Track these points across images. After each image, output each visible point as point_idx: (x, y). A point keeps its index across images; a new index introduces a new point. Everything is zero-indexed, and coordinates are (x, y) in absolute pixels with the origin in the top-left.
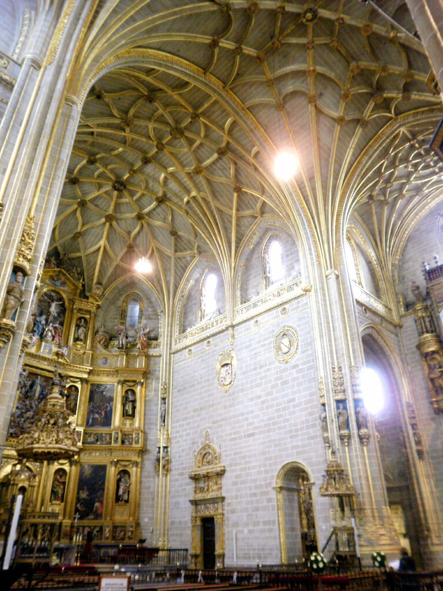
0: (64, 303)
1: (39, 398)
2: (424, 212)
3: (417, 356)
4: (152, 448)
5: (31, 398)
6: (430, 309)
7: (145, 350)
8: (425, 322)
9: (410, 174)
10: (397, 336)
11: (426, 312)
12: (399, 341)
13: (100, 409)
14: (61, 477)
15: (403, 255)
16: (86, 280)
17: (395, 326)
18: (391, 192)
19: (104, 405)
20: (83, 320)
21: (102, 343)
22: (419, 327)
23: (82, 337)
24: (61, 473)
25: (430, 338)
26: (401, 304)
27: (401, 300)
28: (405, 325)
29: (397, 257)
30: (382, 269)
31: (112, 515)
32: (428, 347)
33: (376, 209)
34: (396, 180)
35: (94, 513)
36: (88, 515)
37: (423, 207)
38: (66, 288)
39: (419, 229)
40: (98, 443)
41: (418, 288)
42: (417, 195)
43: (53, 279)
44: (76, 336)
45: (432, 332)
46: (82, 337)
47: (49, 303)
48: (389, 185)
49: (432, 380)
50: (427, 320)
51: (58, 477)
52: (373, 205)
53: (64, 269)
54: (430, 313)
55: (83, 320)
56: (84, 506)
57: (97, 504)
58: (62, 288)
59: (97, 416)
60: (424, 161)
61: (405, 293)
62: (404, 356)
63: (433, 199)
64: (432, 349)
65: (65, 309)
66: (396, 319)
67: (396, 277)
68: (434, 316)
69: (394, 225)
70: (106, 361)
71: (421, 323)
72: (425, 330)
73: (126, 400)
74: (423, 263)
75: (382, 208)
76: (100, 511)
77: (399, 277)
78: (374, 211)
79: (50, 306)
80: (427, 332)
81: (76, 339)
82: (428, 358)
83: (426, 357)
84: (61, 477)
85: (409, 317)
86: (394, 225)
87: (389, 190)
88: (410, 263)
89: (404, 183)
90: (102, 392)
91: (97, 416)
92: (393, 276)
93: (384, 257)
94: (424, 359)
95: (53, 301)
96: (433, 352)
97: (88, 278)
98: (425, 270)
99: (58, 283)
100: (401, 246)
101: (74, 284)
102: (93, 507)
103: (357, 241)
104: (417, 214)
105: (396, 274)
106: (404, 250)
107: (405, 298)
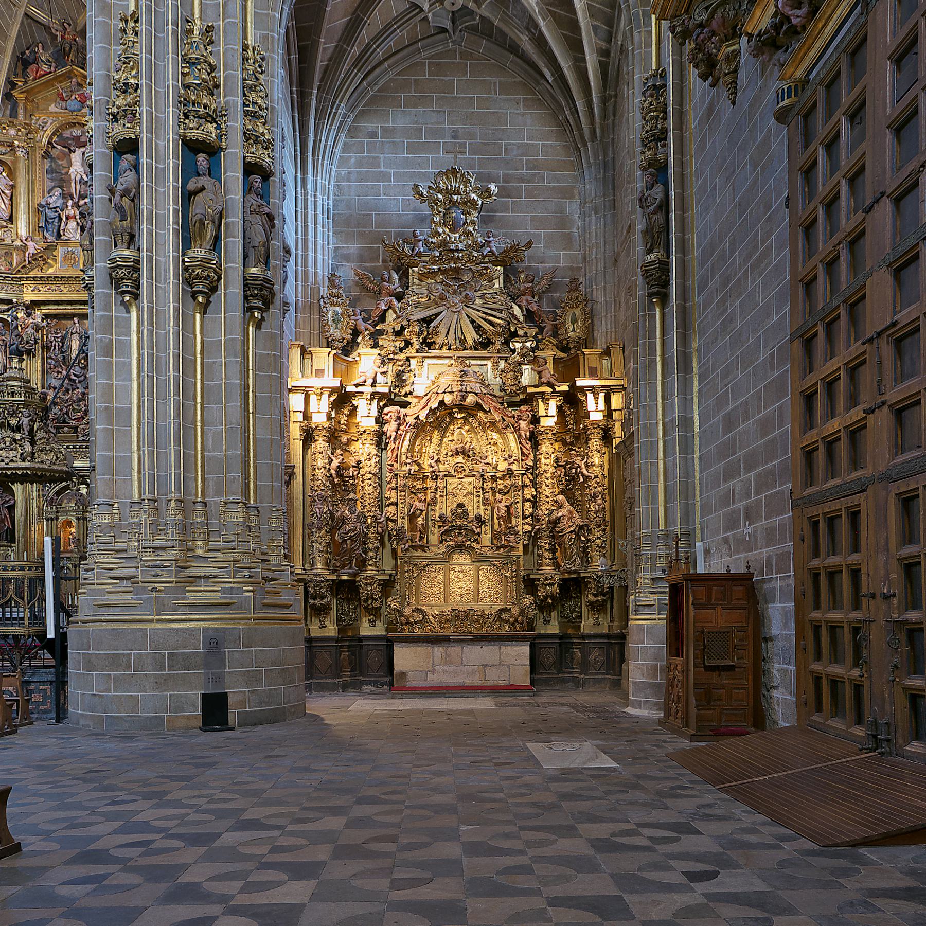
43: (63, 99)
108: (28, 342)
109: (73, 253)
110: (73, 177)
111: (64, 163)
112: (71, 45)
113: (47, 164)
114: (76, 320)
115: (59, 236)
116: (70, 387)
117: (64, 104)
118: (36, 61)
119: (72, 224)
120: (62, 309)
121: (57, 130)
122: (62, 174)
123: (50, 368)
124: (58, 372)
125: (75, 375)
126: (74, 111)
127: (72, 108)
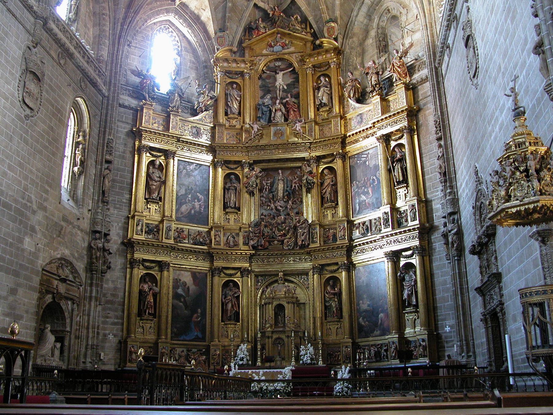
0: (294, 68)
1: (284, 197)
4: (438, 221)
5: (274, 199)
7: (408, 79)
13: (365, 188)
14: (333, 288)
16: (314, 26)
19: (369, 180)
20: (322, 78)
21: (352, 95)
23: (325, 100)
24: (331, 282)
31: (401, 329)
35: (380, 330)
36: (372, 331)
38: (292, 49)
40: (369, 234)
44: (318, 103)
46: (325, 100)
47: (274, 76)
51: (329, 288)
53: (278, 27)
55: (322, 78)
56: (367, 321)
57: (381, 315)
58: (286, 51)
59: (363, 197)
65: (297, 74)
70: (361, 118)
73: (393, 163)
76: (386, 324)
79: (275, 80)
81: (318, 107)
84: (333, 288)
90: (365, 162)
91: (363, 197)
95: (276, 73)
97: (317, 22)
99: (277, 48)
101: (301, 39)
102: (378, 320)
108: (252, 186)
109: (280, 130)
110: (278, 87)
111: (270, 81)
112: (278, 17)
113: (260, 82)
114: (280, 171)
115: (270, 121)
116: (275, 215)
117: (272, 49)
118: (257, 28)
119: (279, 114)
120: (271, 165)
121: (267, 63)
122: (269, 87)
123: (263, 203)
124: (268, 205)
125: (281, 206)
126: (278, 52)
127: (277, 50)
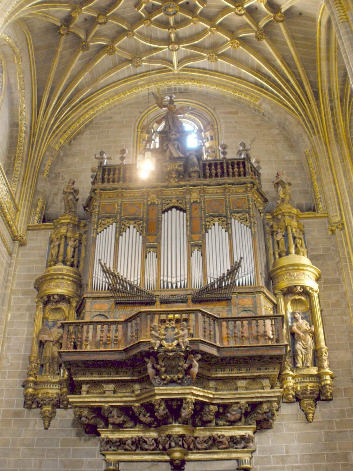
2: (126, 97)
3: (31, 300)
6: (82, 230)
8: (66, 245)
9: (139, 20)
10: (10, 255)
11: (74, 231)
12: (10, 265)
15: (70, 143)
17: (14, 239)
18: (97, 35)
22: (54, 252)
25: (65, 272)
26: (38, 209)
27: (40, 204)
28: (30, 244)
29: (62, 141)
30: (31, 144)
32: (57, 286)
33: (64, 49)
34: (115, 16)
37: (130, 89)
39: (111, 118)
41: (76, 191)
42: (131, 61)
45: (72, 265)
48: (101, 19)
49: (42, 344)
50: (71, 243)
52: (63, 38)
54: (81, 235)
60: (165, 10)
61: (50, 200)
62: (8, 291)
63: (149, 83)
64: (60, 291)
66: (20, 227)
67: (47, 168)
68: (84, 243)
69: (78, 91)
71: (59, 245)
72: (61, 258)
74: (102, 153)
75: (74, 53)
77: (51, 171)
78: (60, 50)
80: (64, 262)
82: (49, 306)
83: (46, 303)
85: (43, 232)
86: (78, 91)
87: (97, 28)
88: (77, 159)
89: (124, 30)
92: (42, 164)
93: (40, 129)
94: (41, 306)
96: (62, 298)
98: (101, 163)
100: (74, 127)
103: (12, 81)
104: (117, 94)
105: (49, 163)
106: (74, 138)
107: (46, 206)
